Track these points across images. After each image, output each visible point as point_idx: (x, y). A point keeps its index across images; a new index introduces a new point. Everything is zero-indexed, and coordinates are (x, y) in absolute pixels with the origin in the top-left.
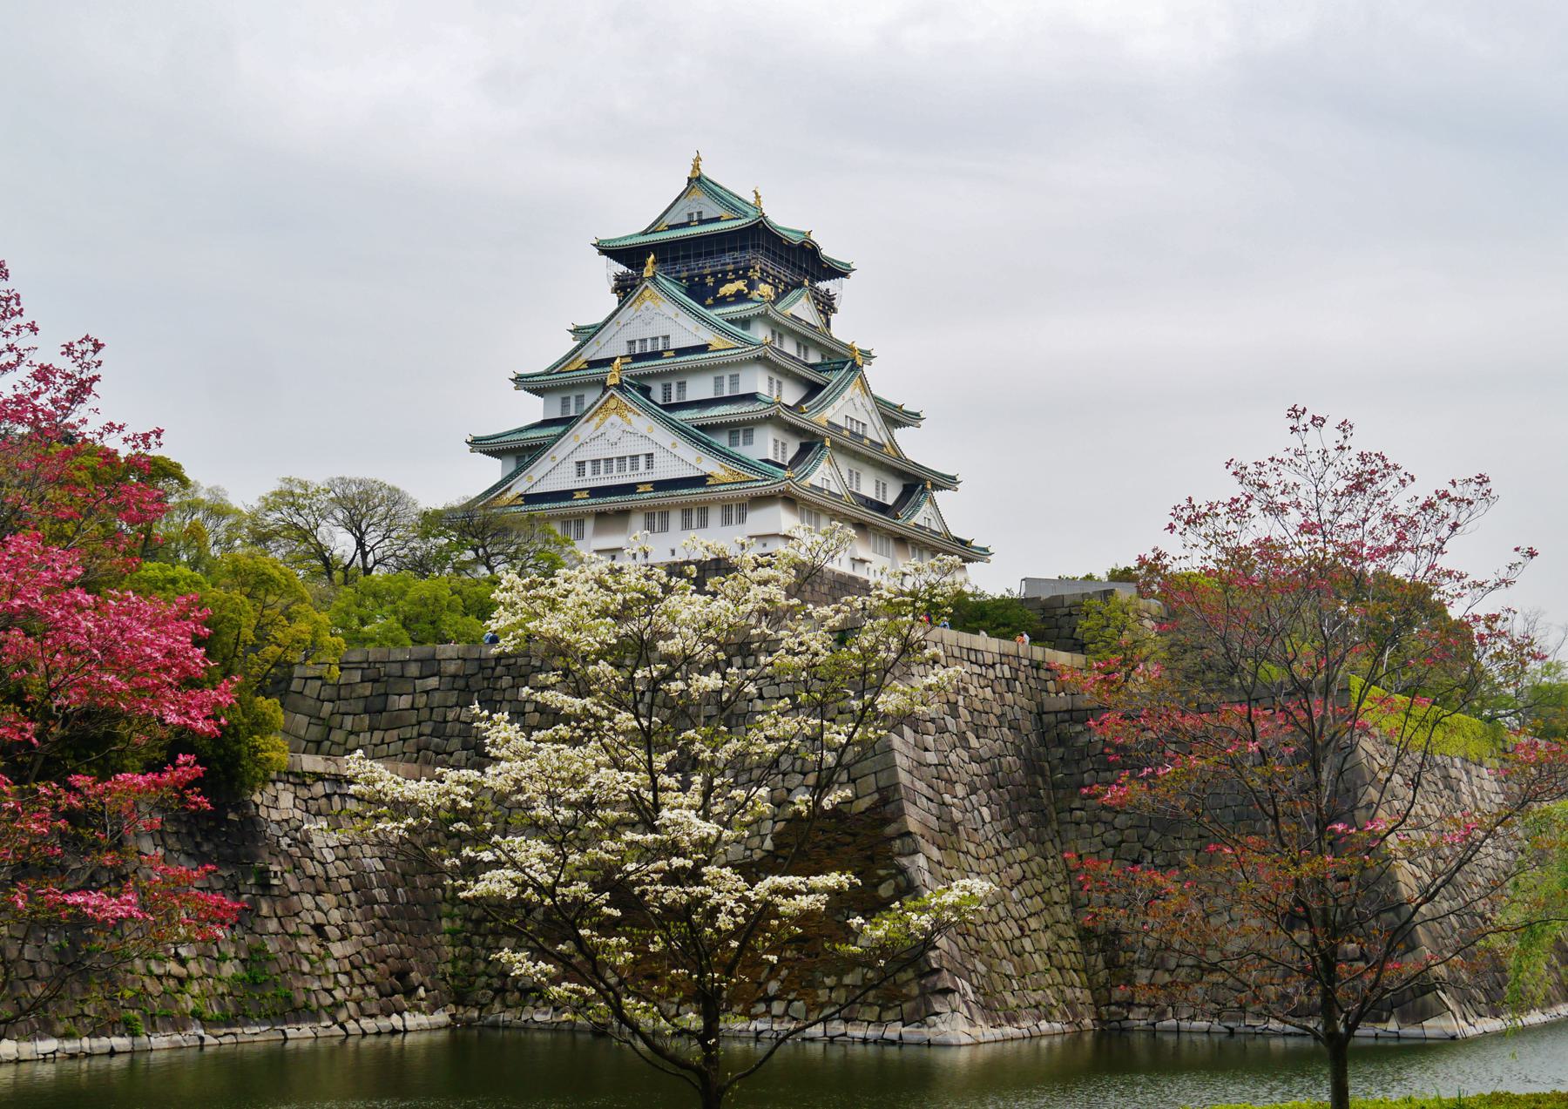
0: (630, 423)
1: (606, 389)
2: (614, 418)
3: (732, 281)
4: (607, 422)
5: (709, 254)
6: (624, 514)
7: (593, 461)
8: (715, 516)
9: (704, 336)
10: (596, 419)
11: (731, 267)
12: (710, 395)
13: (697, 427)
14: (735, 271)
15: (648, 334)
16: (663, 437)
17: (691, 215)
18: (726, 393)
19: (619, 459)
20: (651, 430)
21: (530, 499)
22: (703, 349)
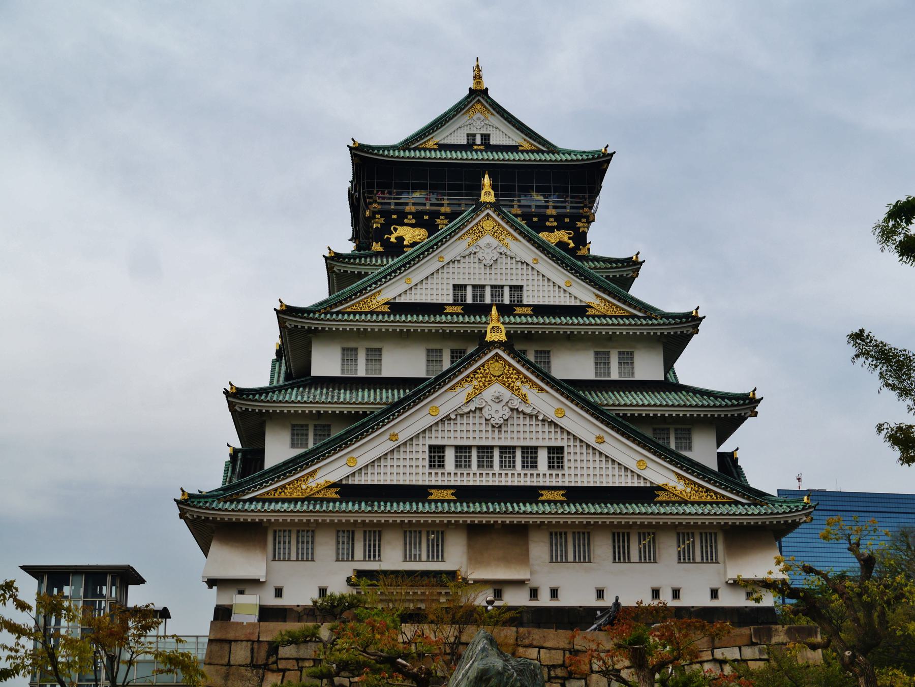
0: (524, 399)
1: (485, 346)
2: (497, 389)
3: (551, 230)
8: (668, 549)
10: (469, 389)
14: (558, 218)
15: (488, 279)
16: (583, 426)
17: (471, 136)
18: (615, 375)
19: (503, 449)
20: (561, 413)
21: (347, 491)
22: (580, 311)
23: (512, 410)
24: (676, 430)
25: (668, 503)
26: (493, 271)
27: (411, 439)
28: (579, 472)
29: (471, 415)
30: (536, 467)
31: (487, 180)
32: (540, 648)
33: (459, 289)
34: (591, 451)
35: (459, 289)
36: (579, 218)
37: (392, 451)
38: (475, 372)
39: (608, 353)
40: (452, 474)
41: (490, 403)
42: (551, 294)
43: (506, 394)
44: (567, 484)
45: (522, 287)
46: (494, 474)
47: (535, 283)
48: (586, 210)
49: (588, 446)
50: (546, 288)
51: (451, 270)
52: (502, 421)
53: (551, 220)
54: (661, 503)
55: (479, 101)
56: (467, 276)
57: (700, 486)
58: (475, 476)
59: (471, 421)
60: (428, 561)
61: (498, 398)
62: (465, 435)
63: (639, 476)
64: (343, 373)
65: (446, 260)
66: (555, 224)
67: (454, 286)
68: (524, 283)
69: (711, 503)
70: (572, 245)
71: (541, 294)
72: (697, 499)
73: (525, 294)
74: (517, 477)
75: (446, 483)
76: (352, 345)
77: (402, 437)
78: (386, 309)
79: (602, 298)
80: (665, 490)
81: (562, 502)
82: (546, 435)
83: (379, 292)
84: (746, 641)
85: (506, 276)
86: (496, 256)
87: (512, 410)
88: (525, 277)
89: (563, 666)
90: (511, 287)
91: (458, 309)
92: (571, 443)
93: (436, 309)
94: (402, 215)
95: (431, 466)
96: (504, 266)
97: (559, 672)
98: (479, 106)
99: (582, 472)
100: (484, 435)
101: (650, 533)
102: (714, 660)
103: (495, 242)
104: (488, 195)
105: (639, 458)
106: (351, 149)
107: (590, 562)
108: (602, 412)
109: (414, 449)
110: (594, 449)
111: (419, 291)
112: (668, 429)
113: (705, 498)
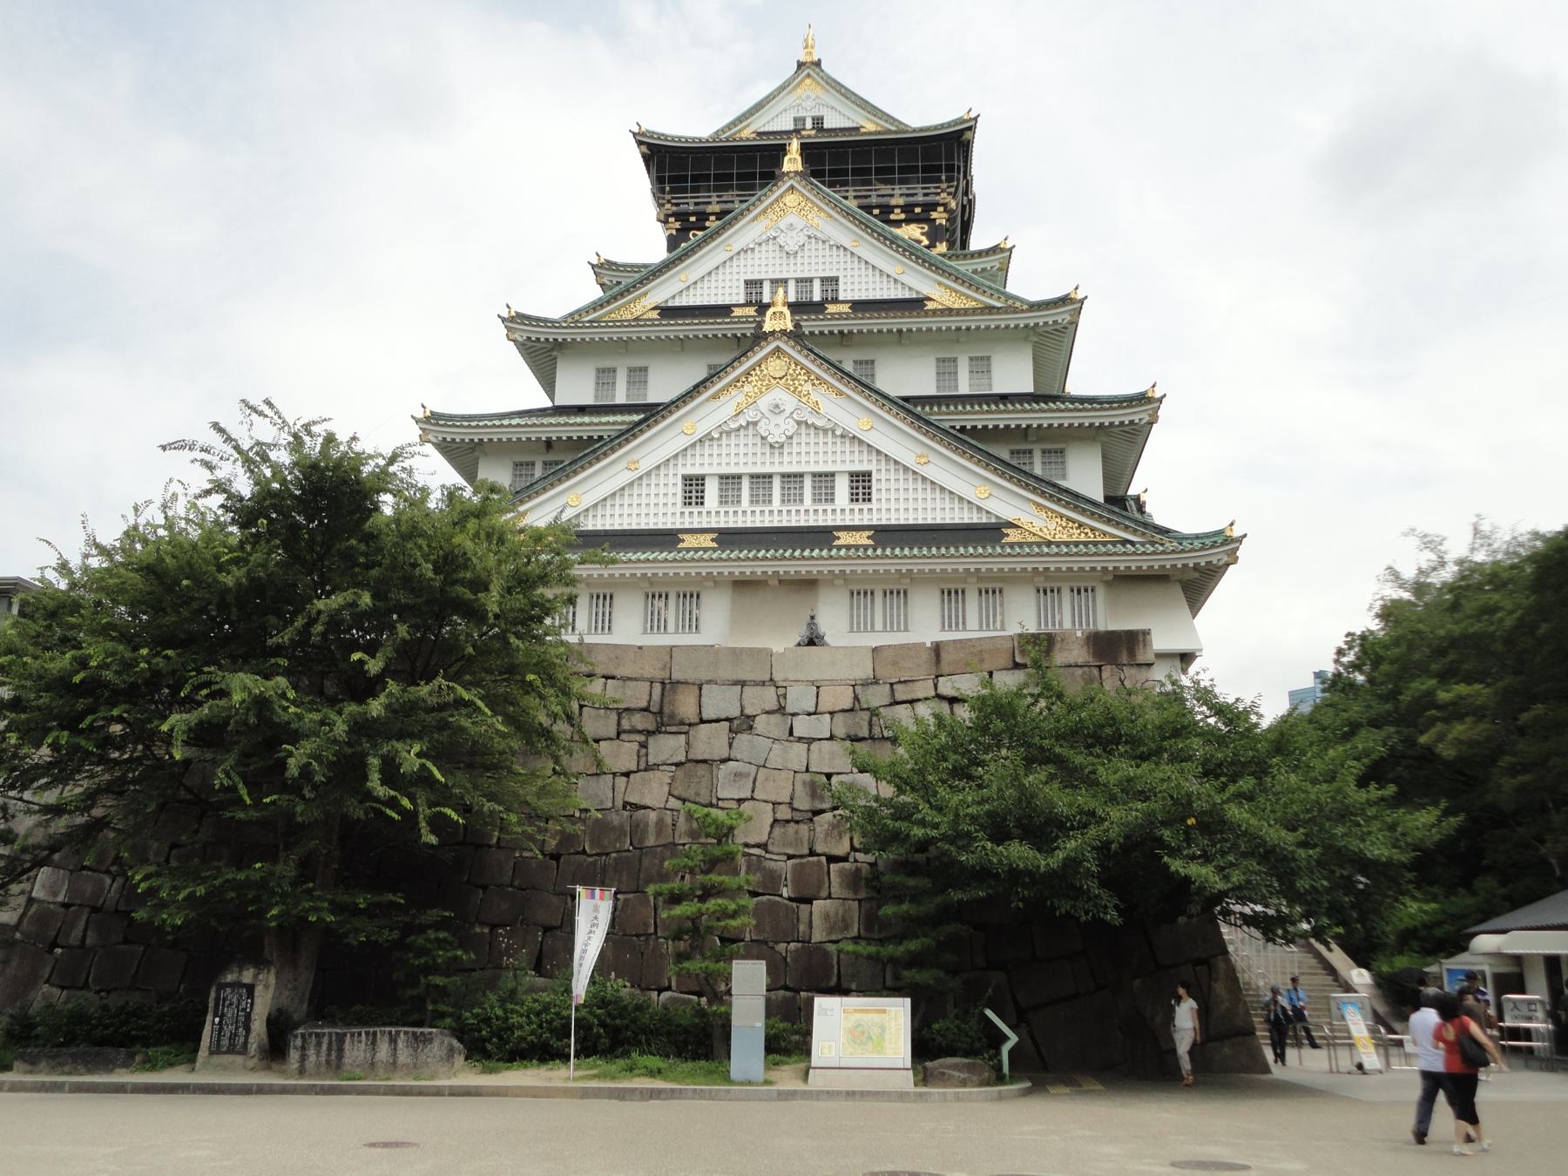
0: (816, 411)
1: (760, 337)
2: (779, 395)
3: (897, 223)
4: (764, 403)
5: (862, 176)
6: (808, 585)
7: (723, 478)
9: (920, 282)
11: (901, 201)
12: (931, 390)
13: (963, 429)
14: (907, 208)
16: (897, 441)
18: (964, 388)
22: (916, 305)
23: (799, 423)
24: (1044, 452)
25: (1021, 545)
26: (799, 260)
27: (658, 467)
28: (893, 506)
29: (742, 432)
30: (833, 500)
31: (795, 146)
32: (607, 678)
33: (753, 285)
34: (910, 477)
35: (753, 285)
36: (933, 206)
37: (631, 484)
38: (748, 374)
39: (955, 360)
40: (715, 513)
41: (768, 414)
42: (878, 286)
43: (789, 402)
44: (875, 522)
45: (836, 279)
46: (771, 512)
47: (856, 272)
48: (944, 195)
49: (906, 469)
50: (871, 279)
51: (742, 262)
52: (784, 439)
53: (897, 211)
54: (1012, 545)
55: (809, 75)
56: (764, 269)
57: (1069, 519)
58: (747, 515)
59: (742, 441)
60: (677, 632)
61: (777, 406)
62: (733, 460)
63: (979, 509)
64: (596, 397)
65: (736, 248)
66: (903, 216)
67: (746, 282)
68: (840, 274)
69: (1086, 544)
70: (926, 242)
71: (864, 287)
72: (1065, 538)
73: (841, 287)
74: (806, 513)
75: (705, 526)
76: (607, 363)
77: (644, 466)
78: (655, 315)
79: (947, 287)
80: (1016, 527)
81: (866, 548)
82: (848, 457)
83: (645, 294)
84: (1005, 660)
85: (815, 265)
86: (802, 239)
87: (799, 423)
88: (842, 266)
89: (646, 710)
90: (823, 280)
91: (751, 311)
92: (883, 466)
93: (724, 310)
94: (703, 217)
95: (687, 502)
96: (814, 253)
97: (639, 721)
98: (808, 81)
99: (896, 504)
100: (759, 459)
101: (993, 588)
102: (939, 697)
103: (799, 222)
104: (792, 162)
105: (976, 482)
106: (635, 135)
107: (906, 630)
108: (928, 423)
109: (662, 481)
110: (914, 473)
111: (699, 292)
112: (1031, 452)
113: (1076, 535)
